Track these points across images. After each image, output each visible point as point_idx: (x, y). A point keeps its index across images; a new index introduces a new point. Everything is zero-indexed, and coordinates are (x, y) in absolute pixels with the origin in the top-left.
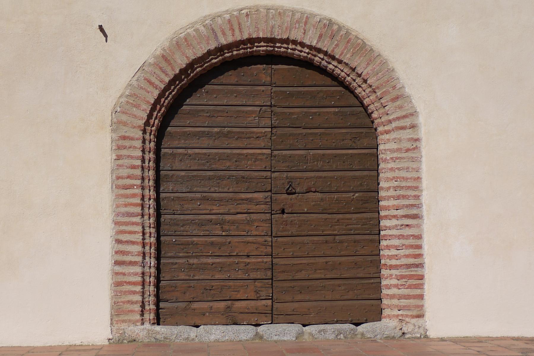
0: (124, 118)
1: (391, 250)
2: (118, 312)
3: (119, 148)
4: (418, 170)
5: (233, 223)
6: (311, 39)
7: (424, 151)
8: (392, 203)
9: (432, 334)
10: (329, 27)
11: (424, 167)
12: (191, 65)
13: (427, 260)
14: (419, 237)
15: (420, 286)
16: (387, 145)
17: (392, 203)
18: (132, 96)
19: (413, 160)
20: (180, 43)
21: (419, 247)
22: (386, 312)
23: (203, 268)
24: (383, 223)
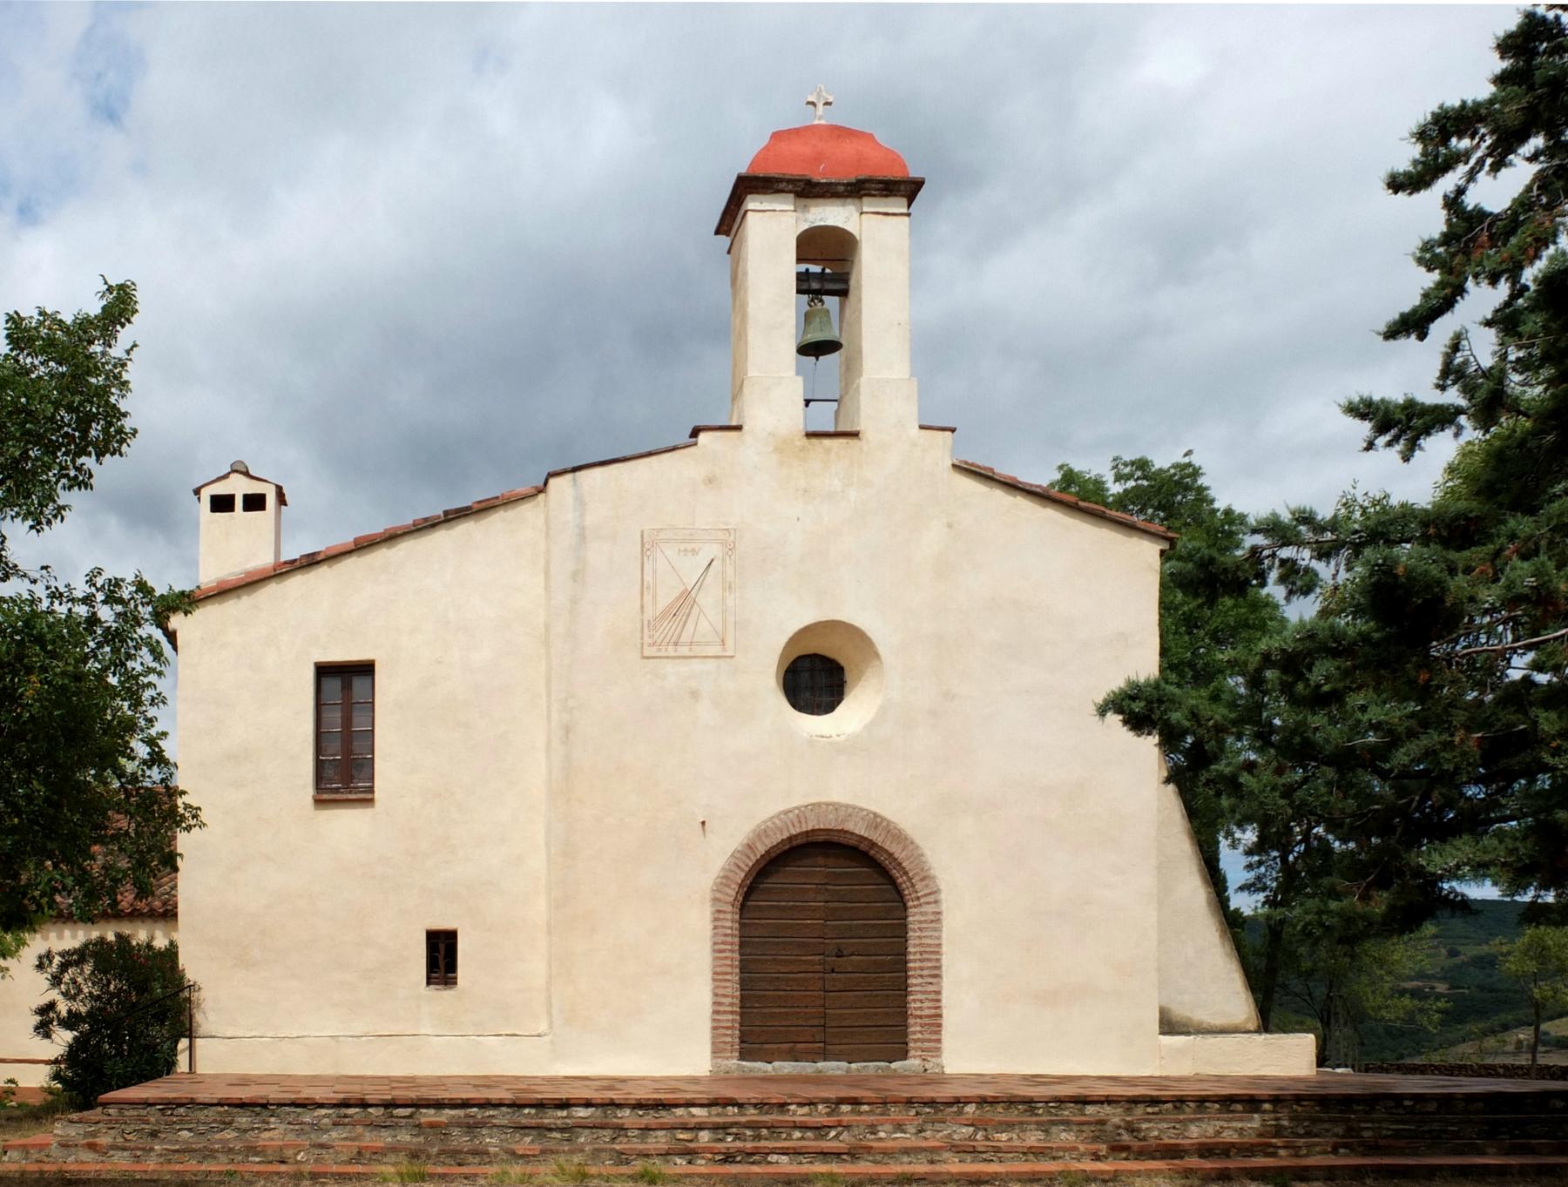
1: (917, 1003)
2: (716, 1051)
3: (716, 920)
4: (939, 938)
5: (794, 980)
6: (861, 831)
7: (944, 923)
8: (918, 964)
9: (948, 1070)
10: (876, 820)
11: (944, 935)
12: (768, 852)
13: (945, 1012)
14: (938, 993)
15: (939, 1032)
16: (914, 918)
17: (918, 964)
18: (725, 879)
19: (935, 930)
20: (760, 834)
21: (939, 1001)
22: (912, 1053)
23: (772, 1015)
24: (910, 981)
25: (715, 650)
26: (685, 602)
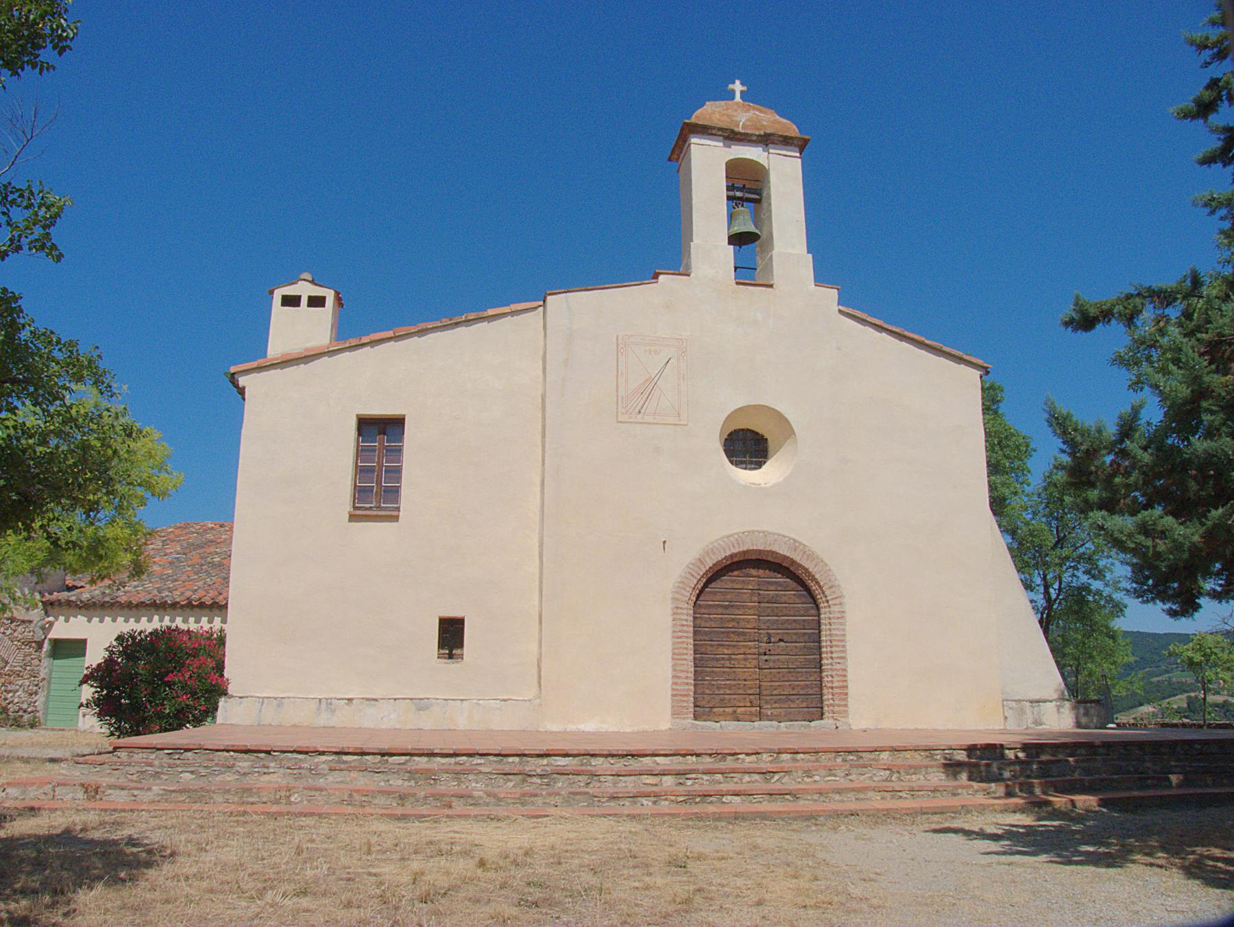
0: (677, 596)
2: (676, 713)
14: (845, 670)
19: (841, 624)
22: (826, 715)
25: (671, 420)
26: (650, 386)
